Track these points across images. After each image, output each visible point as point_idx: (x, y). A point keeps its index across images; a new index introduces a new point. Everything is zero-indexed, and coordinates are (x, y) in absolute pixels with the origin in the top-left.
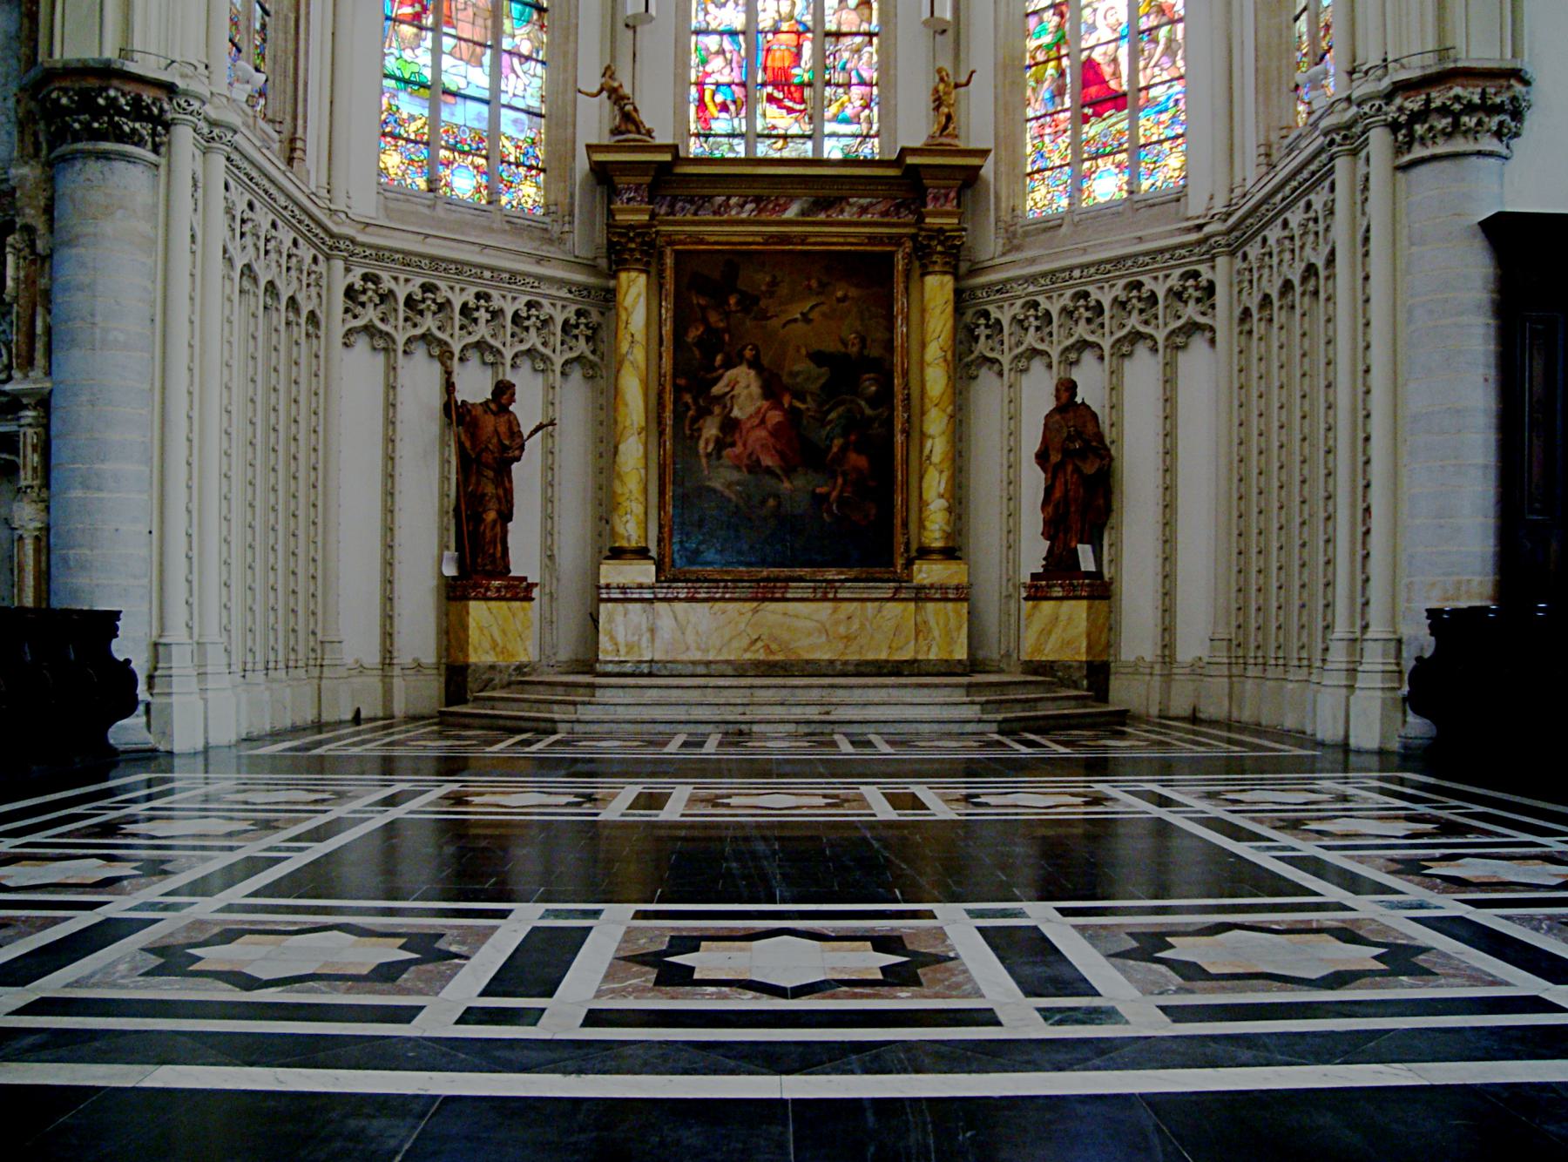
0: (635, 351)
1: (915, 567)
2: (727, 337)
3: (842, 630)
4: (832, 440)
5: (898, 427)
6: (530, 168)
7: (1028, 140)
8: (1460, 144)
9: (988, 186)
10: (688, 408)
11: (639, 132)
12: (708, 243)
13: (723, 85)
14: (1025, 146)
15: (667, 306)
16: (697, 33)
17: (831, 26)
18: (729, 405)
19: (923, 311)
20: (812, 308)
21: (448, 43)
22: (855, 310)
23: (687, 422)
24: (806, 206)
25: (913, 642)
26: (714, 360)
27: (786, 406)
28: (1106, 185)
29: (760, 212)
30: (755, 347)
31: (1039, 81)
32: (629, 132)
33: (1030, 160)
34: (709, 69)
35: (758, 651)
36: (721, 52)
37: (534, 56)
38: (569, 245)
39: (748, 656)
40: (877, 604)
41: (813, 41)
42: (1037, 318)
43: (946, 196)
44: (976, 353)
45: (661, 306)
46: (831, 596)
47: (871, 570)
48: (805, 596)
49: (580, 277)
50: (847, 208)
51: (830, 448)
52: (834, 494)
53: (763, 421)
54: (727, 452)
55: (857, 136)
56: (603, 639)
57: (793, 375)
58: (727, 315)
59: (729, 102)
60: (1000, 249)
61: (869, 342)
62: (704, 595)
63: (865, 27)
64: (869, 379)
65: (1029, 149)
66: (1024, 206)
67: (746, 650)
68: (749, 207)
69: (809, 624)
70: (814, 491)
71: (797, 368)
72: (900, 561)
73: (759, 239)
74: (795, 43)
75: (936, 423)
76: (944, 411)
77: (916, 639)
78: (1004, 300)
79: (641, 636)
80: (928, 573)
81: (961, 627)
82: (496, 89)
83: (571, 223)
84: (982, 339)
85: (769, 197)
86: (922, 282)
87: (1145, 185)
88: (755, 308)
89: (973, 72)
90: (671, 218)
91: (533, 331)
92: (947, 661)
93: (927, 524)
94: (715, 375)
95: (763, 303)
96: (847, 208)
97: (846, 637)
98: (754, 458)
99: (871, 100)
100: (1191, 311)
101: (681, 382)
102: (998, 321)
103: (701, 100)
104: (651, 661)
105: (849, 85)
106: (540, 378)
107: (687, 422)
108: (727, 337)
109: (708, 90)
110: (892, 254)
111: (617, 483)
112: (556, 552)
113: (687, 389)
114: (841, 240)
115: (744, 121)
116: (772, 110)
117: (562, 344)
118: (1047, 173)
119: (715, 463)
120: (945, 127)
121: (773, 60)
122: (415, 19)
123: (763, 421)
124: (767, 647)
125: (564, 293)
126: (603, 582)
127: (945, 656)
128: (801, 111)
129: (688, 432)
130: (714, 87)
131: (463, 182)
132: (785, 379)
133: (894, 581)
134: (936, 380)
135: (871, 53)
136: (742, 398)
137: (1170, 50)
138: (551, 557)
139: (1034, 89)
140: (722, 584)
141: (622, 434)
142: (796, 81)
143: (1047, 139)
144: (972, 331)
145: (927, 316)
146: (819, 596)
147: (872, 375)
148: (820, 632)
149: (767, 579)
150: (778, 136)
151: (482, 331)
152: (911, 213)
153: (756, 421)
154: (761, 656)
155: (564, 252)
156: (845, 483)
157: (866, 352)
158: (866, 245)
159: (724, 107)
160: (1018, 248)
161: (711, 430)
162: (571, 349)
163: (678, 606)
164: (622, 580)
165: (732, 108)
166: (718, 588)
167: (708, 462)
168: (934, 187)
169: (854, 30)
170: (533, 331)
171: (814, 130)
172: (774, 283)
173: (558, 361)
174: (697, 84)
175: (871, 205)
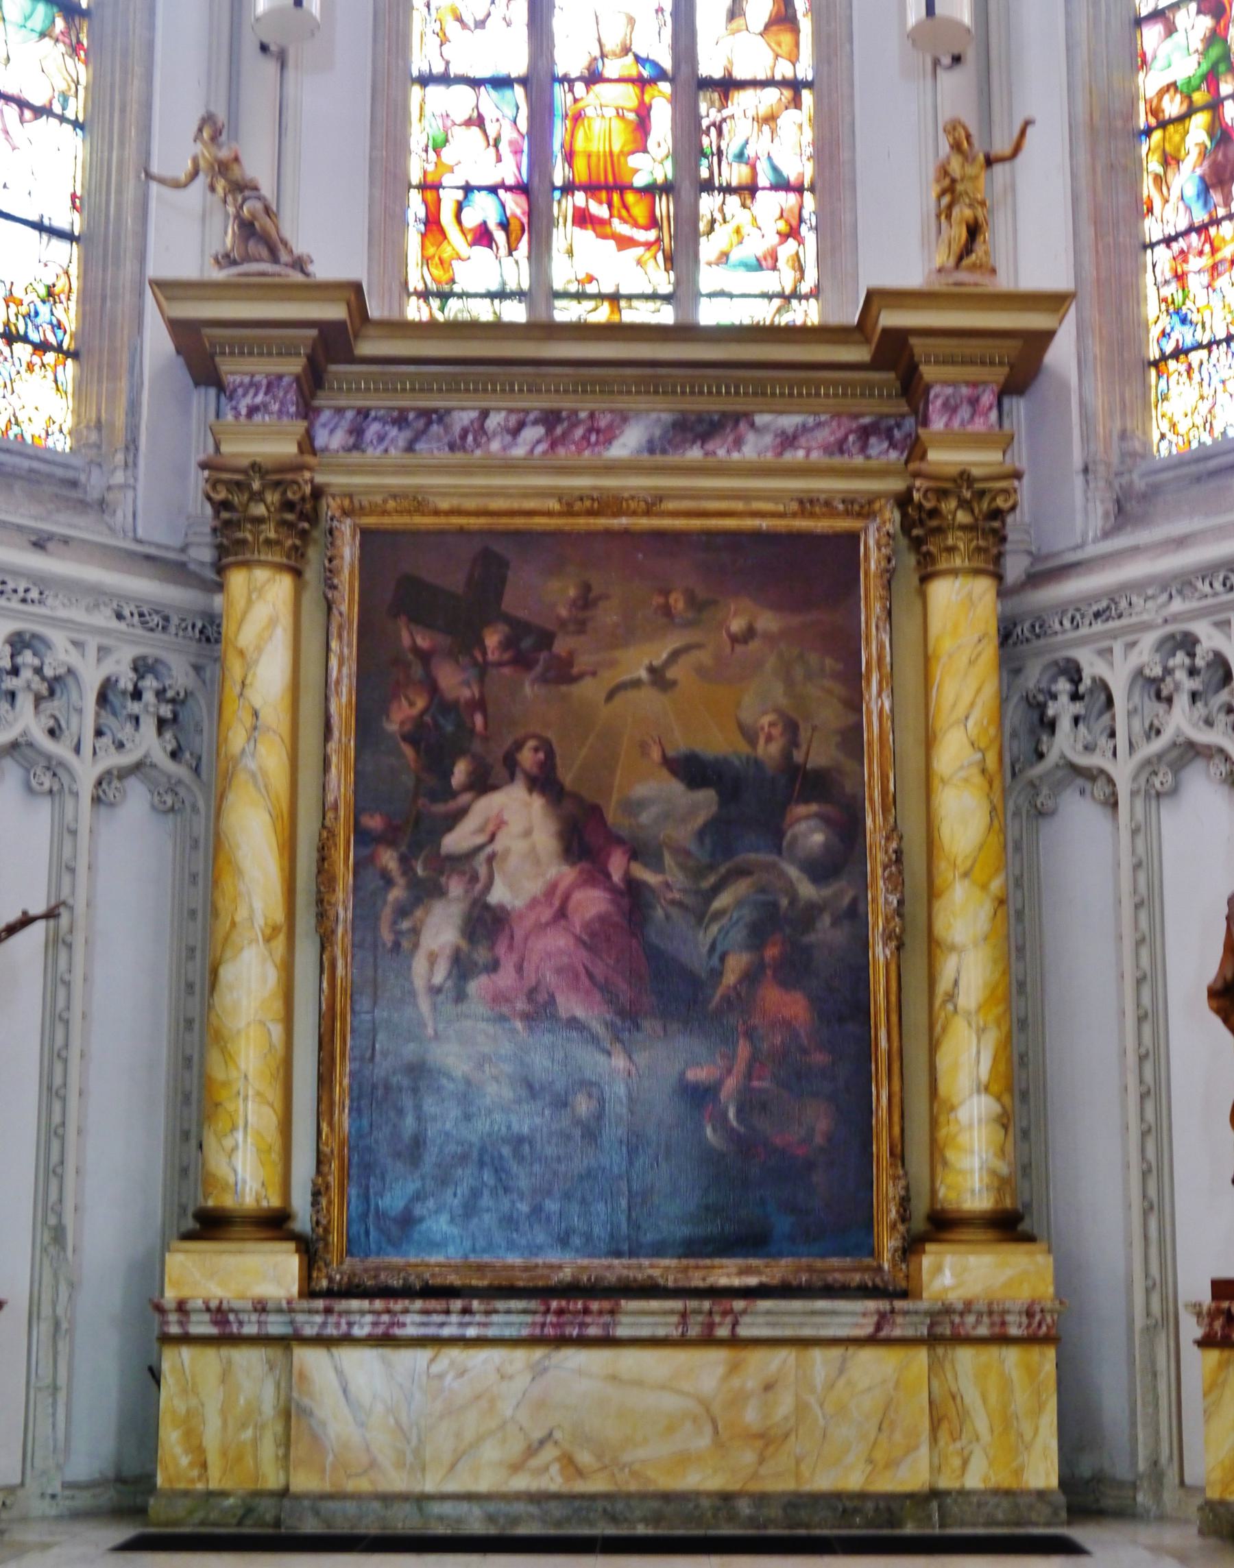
0: (262, 749)
1: (927, 1261)
2: (479, 720)
3: (751, 1416)
4: (722, 958)
5: (877, 925)
6: (42, 347)
7: (1151, 292)
9: (1064, 386)
10: (389, 882)
11: (275, 259)
12: (437, 513)
13: (480, 189)
14: (1139, 299)
15: (344, 651)
16: (425, 80)
17: (709, 67)
18: (483, 871)
19: (927, 661)
20: (675, 655)
22: (771, 662)
23: (387, 913)
24: (658, 432)
25: (924, 1450)
26: (448, 773)
27: (617, 877)
29: (553, 446)
30: (546, 747)
31: (1170, 160)
32: (258, 260)
33: (1155, 332)
34: (448, 155)
35: (546, 1468)
36: (478, 121)
37: (57, 109)
38: (121, 517)
39: (521, 1483)
40: (836, 1353)
41: (674, 100)
42: (1193, 672)
43: (974, 402)
44: (1052, 758)
45: (328, 648)
46: (723, 1332)
47: (819, 1263)
48: (661, 1332)
50: (751, 437)
51: (717, 974)
52: (731, 1084)
53: (562, 914)
54: (477, 986)
55: (769, 297)
56: (171, 1438)
57: (632, 807)
58: (483, 669)
59: (492, 226)
60: (1097, 522)
61: (804, 735)
62: (411, 1331)
63: (784, 70)
64: (808, 817)
65: (1152, 308)
66: (1146, 432)
67: (516, 1468)
68: (532, 433)
69: (670, 1402)
70: (682, 1074)
71: (641, 790)
72: (888, 1244)
73: (553, 505)
74: (634, 103)
76: (984, 887)
77: (934, 1439)
78: (1113, 635)
79: (260, 1427)
81: (1041, 1407)
83: (130, 465)
84: (1065, 725)
85: (575, 412)
86: (923, 596)
88: (543, 656)
89: (1027, 123)
90: (355, 457)
91: (25, 702)
92: (1008, 1493)
93: (951, 1155)
94: (453, 805)
95: (561, 646)
96: (751, 437)
97: (761, 1436)
98: (542, 997)
99: (801, 220)
101: (374, 823)
102: (1102, 686)
103: (432, 223)
104: (284, 1493)
105: (749, 190)
106: (44, 808)
107: (387, 913)
108: (479, 720)
109: (449, 199)
110: (853, 539)
111: (215, 1056)
112: (69, 1220)
113: (389, 837)
114: (739, 506)
115: (524, 264)
116: (585, 237)
117: (99, 733)
118: (1195, 357)
119: (449, 1009)
120: (967, 250)
121: (588, 139)
123: (562, 914)
124: (568, 1463)
125: (106, 618)
126: (170, 1295)
127: (1003, 1479)
128: (648, 245)
129: (387, 936)
130: (459, 195)
132: (612, 815)
133: (865, 1292)
136: (513, 862)
138: (58, 1235)
139: (1159, 180)
140: (457, 1304)
141: (226, 938)
142: (639, 181)
143: (1196, 283)
144: (1042, 707)
145: (937, 672)
146: (693, 1332)
147: (814, 808)
148: (695, 1420)
149: (571, 1290)
150: (600, 297)
152: (893, 445)
153: (546, 914)
154: (554, 1482)
155: (112, 529)
156: (754, 1059)
157: (798, 756)
158: (794, 515)
159: (483, 236)
160: (1141, 520)
162: (120, 746)
163: (349, 1356)
164: (217, 1291)
165: (500, 236)
166: (447, 1312)
167: (434, 1007)
168: (946, 383)
169: (761, 76)
170: (25, 702)
171: (677, 284)
172: (586, 601)
173: (86, 772)
174: (424, 187)
175: (805, 429)
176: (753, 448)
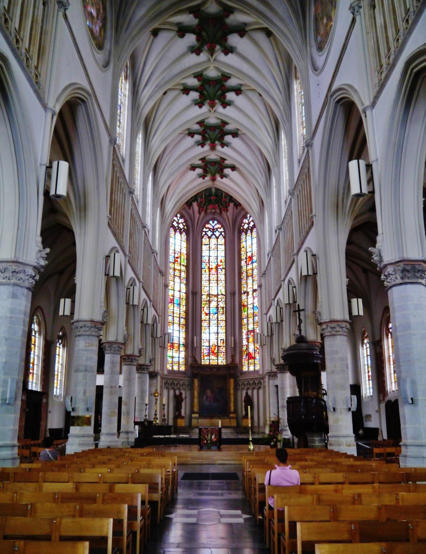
8: (273, 378)
17: (219, 345)
21: (174, 351)
28: (252, 368)
49: (189, 379)
75: (232, 397)
80: (231, 415)
82: (179, 356)
87: (256, 368)
100: (260, 385)
116: (212, 356)
122: (170, 349)
131: (176, 368)
134: (232, 392)
135: (224, 349)
137: (258, 353)
151: (178, 386)
161: (205, 398)
173: (187, 389)
176: (221, 371)
